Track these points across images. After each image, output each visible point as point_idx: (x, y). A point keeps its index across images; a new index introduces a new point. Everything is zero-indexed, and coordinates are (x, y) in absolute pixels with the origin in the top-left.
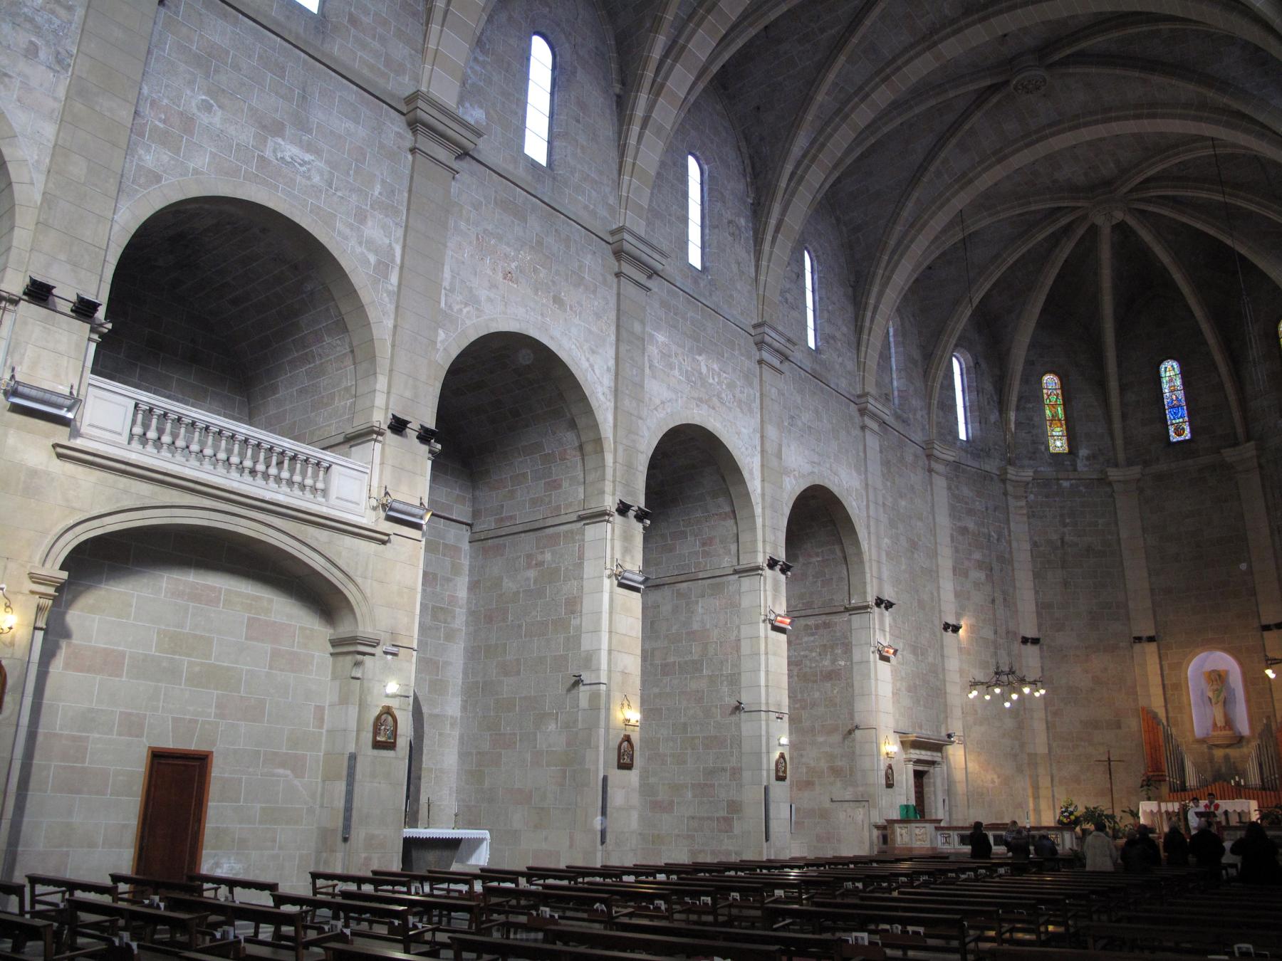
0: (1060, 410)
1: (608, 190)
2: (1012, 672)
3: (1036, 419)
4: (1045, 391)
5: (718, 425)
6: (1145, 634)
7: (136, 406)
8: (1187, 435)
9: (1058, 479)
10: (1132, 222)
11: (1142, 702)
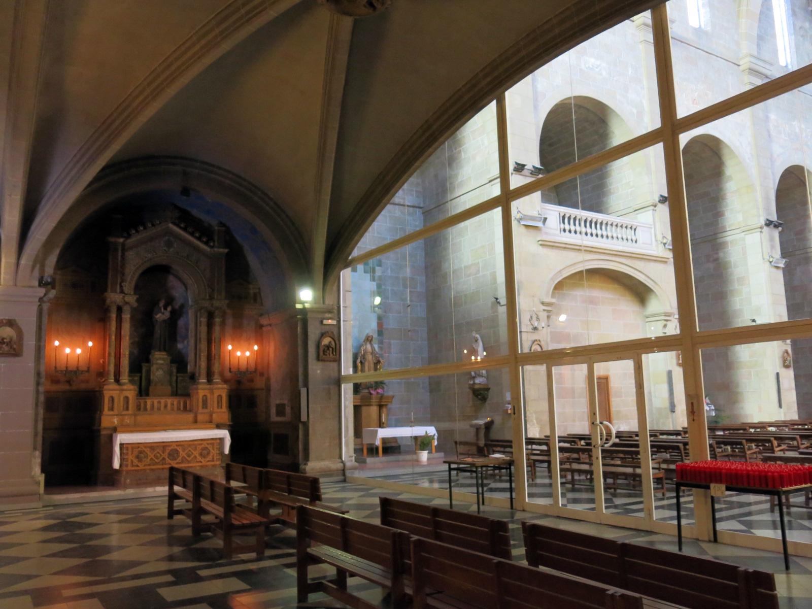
7: (559, 214)
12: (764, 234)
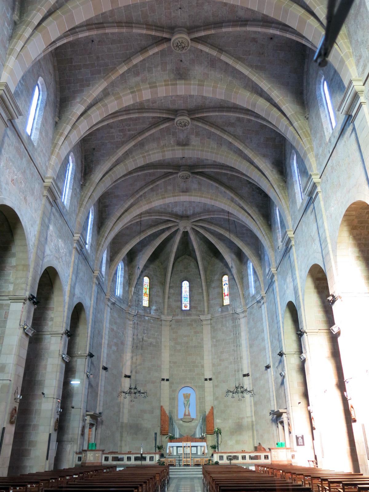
0: (148, 291)
1: (47, 159)
2: (136, 388)
3: (140, 292)
4: (144, 283)
5: (60, 270)
6: (166, 378)
8: (188, 308)
10: (190, 232)
11: (162, 404)
12: (26, 305)
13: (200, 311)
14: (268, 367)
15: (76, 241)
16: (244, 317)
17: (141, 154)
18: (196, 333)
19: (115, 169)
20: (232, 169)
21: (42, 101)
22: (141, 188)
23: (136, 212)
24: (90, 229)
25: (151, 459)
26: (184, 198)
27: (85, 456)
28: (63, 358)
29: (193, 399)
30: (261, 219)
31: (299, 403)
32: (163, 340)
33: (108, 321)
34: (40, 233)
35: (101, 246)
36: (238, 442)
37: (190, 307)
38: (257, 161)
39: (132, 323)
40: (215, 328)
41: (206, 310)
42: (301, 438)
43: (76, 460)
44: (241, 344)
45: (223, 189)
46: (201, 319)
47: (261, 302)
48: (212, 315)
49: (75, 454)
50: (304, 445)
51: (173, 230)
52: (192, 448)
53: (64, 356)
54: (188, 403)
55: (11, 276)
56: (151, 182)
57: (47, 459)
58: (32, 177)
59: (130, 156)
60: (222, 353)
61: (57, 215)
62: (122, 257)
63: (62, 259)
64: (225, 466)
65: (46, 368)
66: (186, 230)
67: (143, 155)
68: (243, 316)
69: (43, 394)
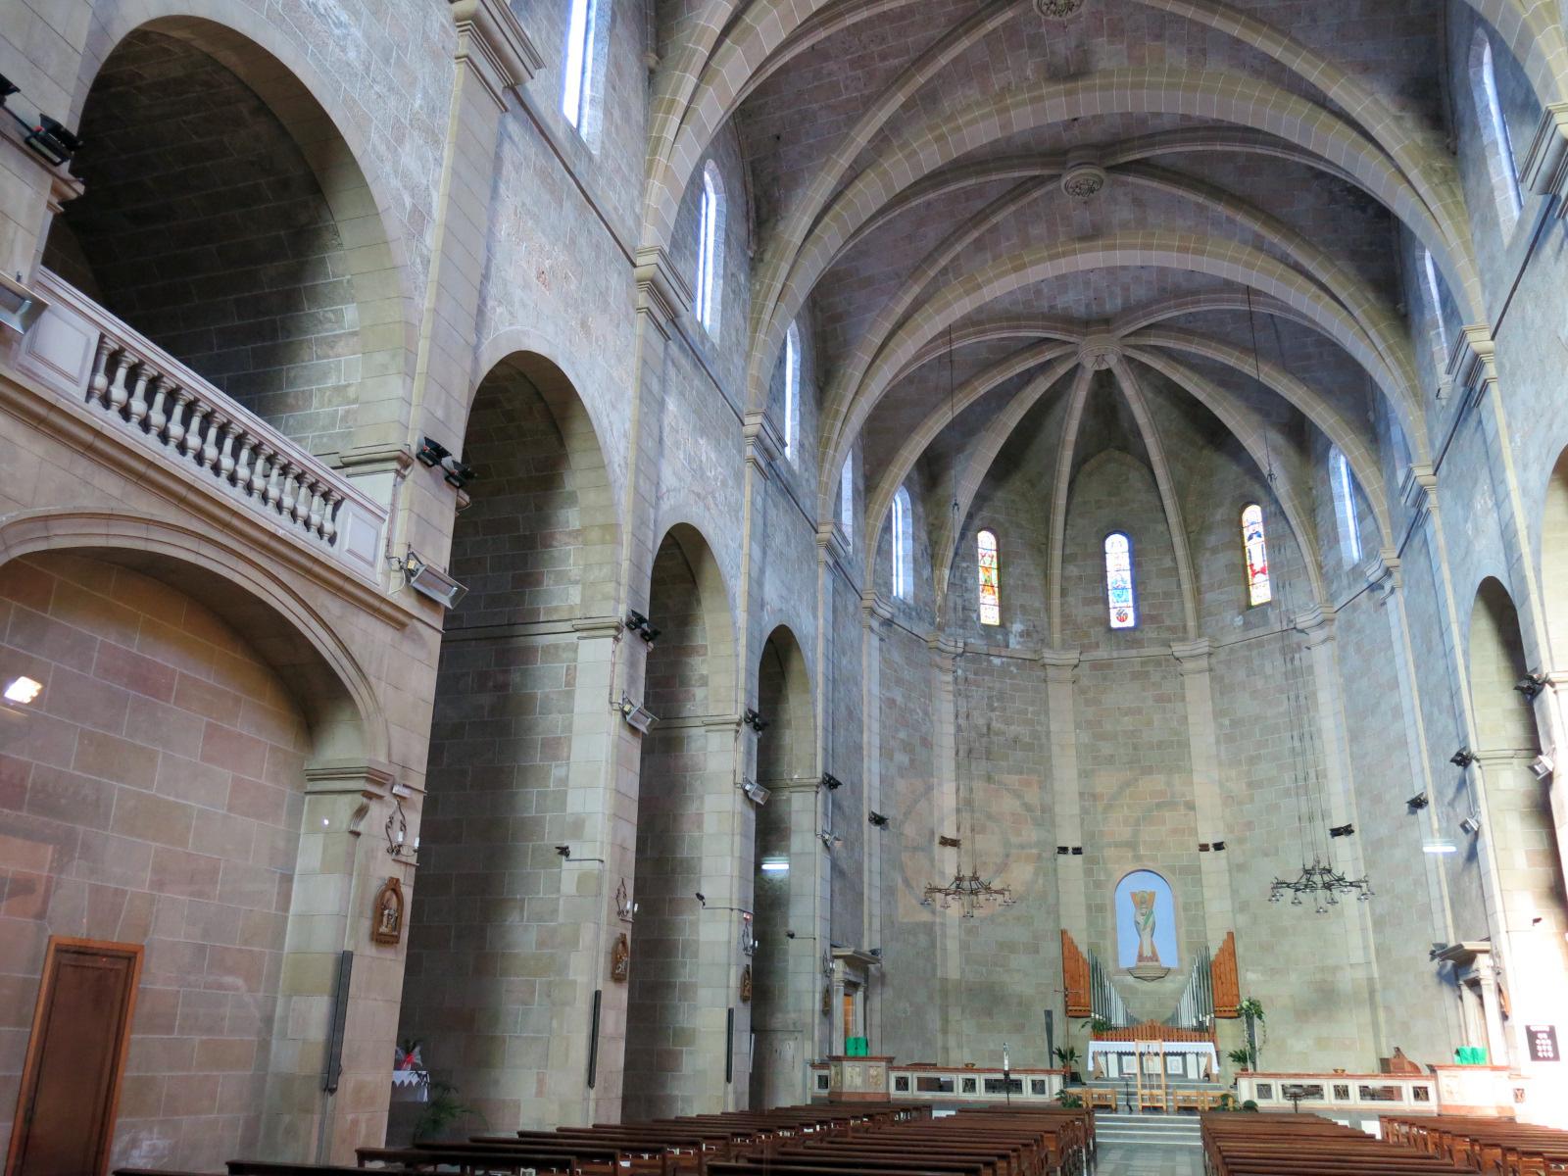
0: (994, 574)
3: (970, 582)
4: (980, 551)
5: (711, 531)
6: (1071, 845)
7: (102, 337)
8: (1130, 622)
9: (989, 655)
10: (1117, 371)
11: (1064, 925)
12: (621, 644)
13: (1172, 629)
14: (1417, 804)
15: (751, 440)
16: (1324, 641)
17: (931, 129)
18: (1161, 699)
19: (849, 194)
20: (1248, 134)
21: (599, 9)
22: (944, 244)
23: (932, 324)
24: (794, 395)
25: (1039, 1087)
26: (1090, 259)
27: (837, 1074)
28: (746, 792)
29: (1164, 909)
30: (1368, 300)
31: (1537, 921)
32: (1053, 727)
33: (876, 676)
34: (640, 424)
35: (833, 445)
36: (1322, 1043)
37: (1138, 617)
38: (1338, 91)
39: (949, 678)
40: (1226, 681)
41: (1191, 623)
42: (1545, 1036)
43: (813, 1084)
44: (1319, 731)
45: (1221, 210)
46: (1176, 654)
47: (1382, 588)
48: (1213, 639)
49: (809, 1069)
50: (1556, 1057)
51: (1061, 370)
52: (1169, 1058)
53: (748, 787)
54: (1148, 919)
55: (571, 561)
56: (970, 220)
57: (729, 1079)
58: (598, 257)
59: (895, 143)
60: (1253, 760)
61: (686, 364)
62: (903, 475)
63: (714, 497)
64: (1277, 1118)
65: (700, 827)
66: (1104, 367)
67: (937, 133)
68: (1322, 637)
69: (700, 897)
